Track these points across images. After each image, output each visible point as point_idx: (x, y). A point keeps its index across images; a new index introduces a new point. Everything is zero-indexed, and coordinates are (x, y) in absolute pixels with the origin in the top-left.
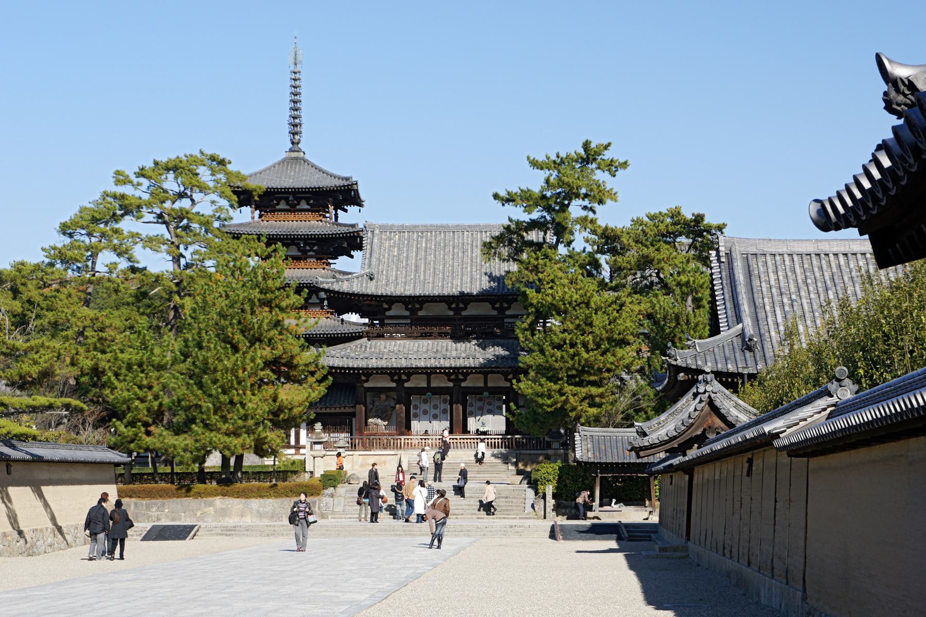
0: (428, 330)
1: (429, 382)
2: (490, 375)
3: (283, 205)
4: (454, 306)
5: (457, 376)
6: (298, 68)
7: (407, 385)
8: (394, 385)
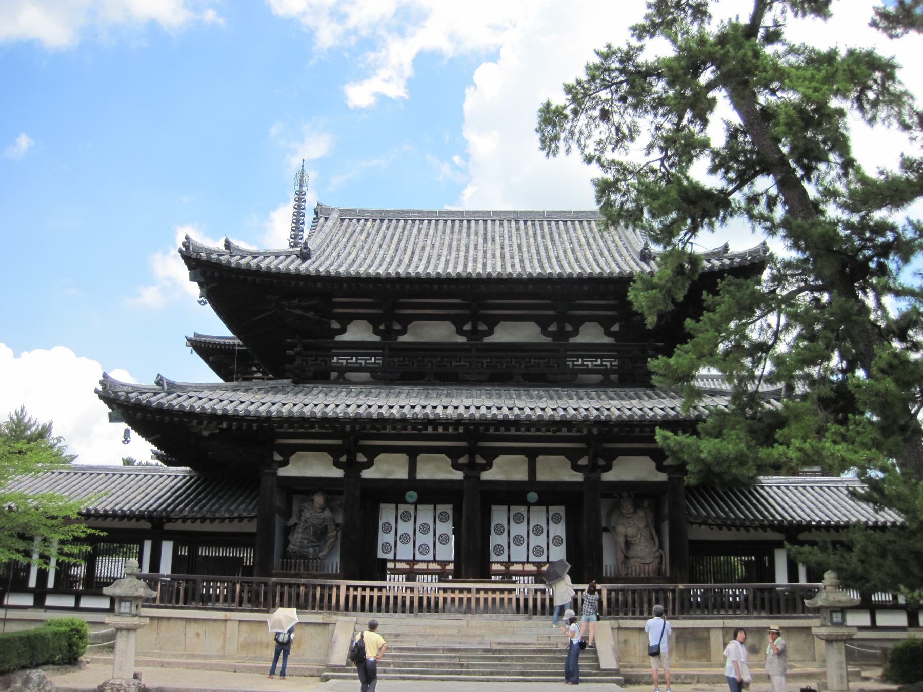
1: (412, 469)
2: (540, 459)
4: (467, 327)
5: (472, 457)
6: (304, 189)
7: (367, 474)
8: (338, 473)
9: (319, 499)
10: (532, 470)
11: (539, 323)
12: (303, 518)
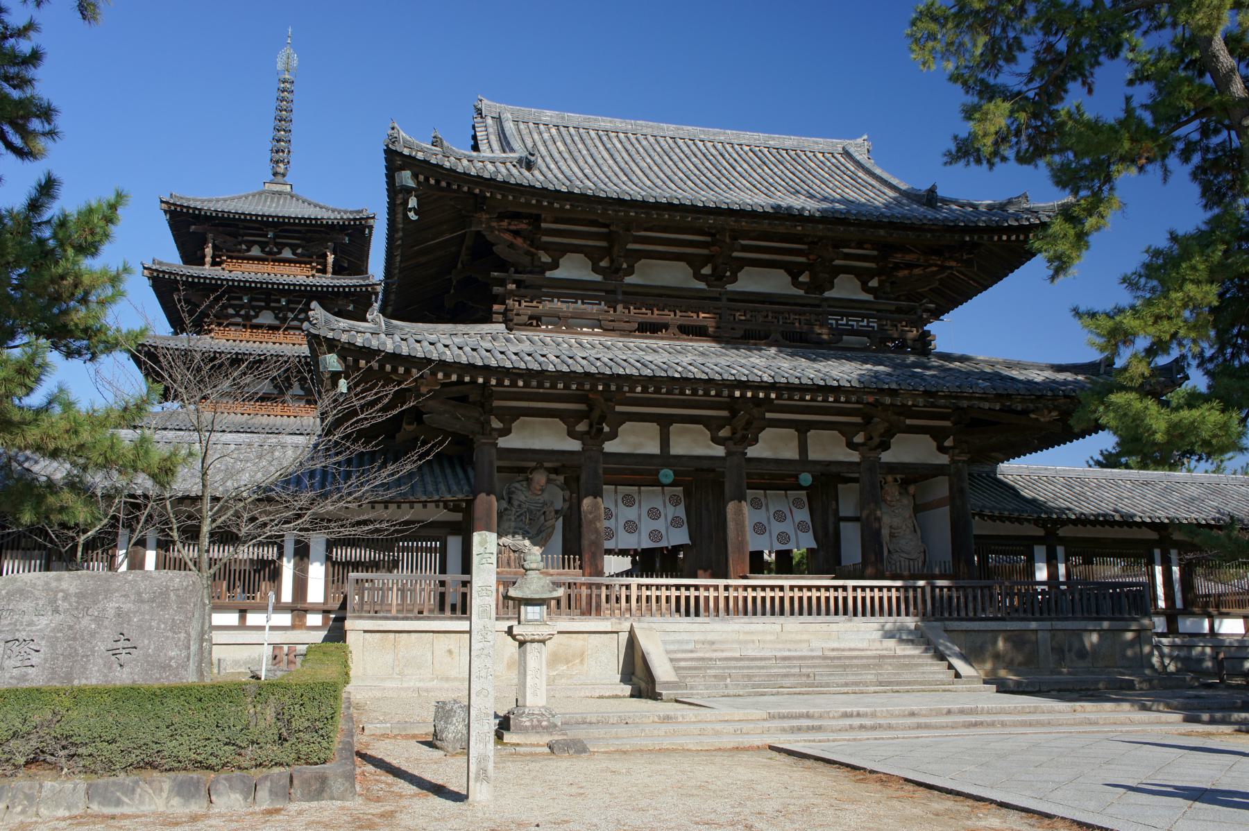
0: (655, 316)
1: (665, 442)
2: (811, 433)
3: (255, 251)
7: (609, 447)
9: (540, 478)
10: (803, 448)
11: (789, 272)
12: (516, 503)
